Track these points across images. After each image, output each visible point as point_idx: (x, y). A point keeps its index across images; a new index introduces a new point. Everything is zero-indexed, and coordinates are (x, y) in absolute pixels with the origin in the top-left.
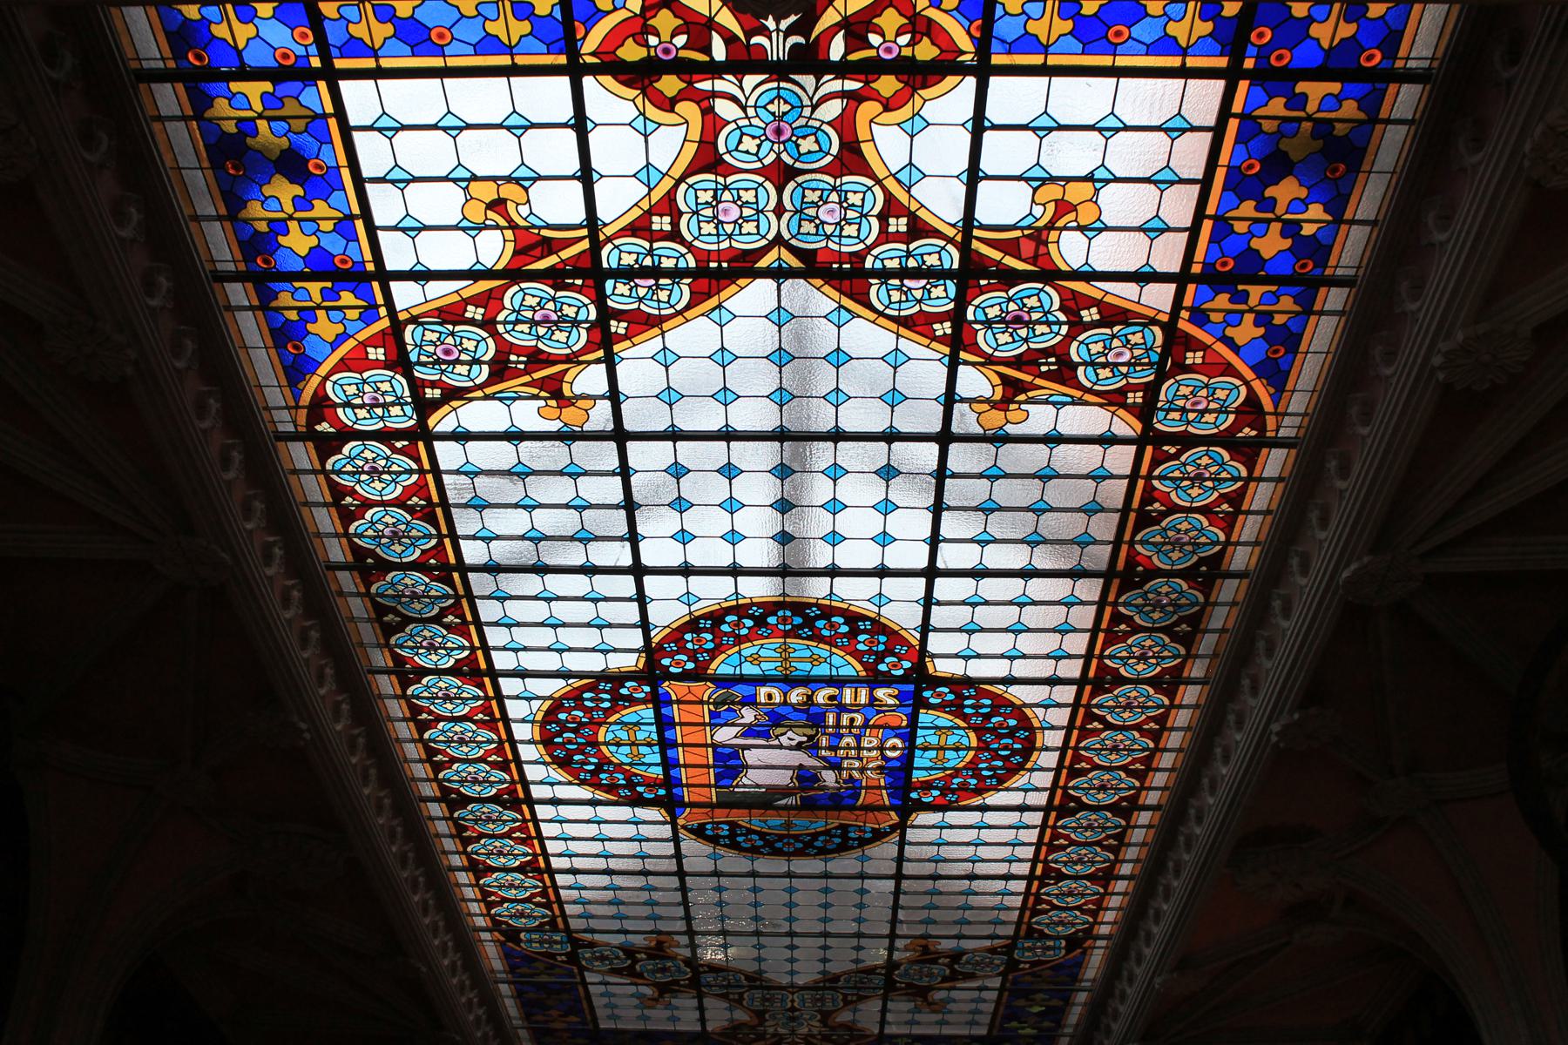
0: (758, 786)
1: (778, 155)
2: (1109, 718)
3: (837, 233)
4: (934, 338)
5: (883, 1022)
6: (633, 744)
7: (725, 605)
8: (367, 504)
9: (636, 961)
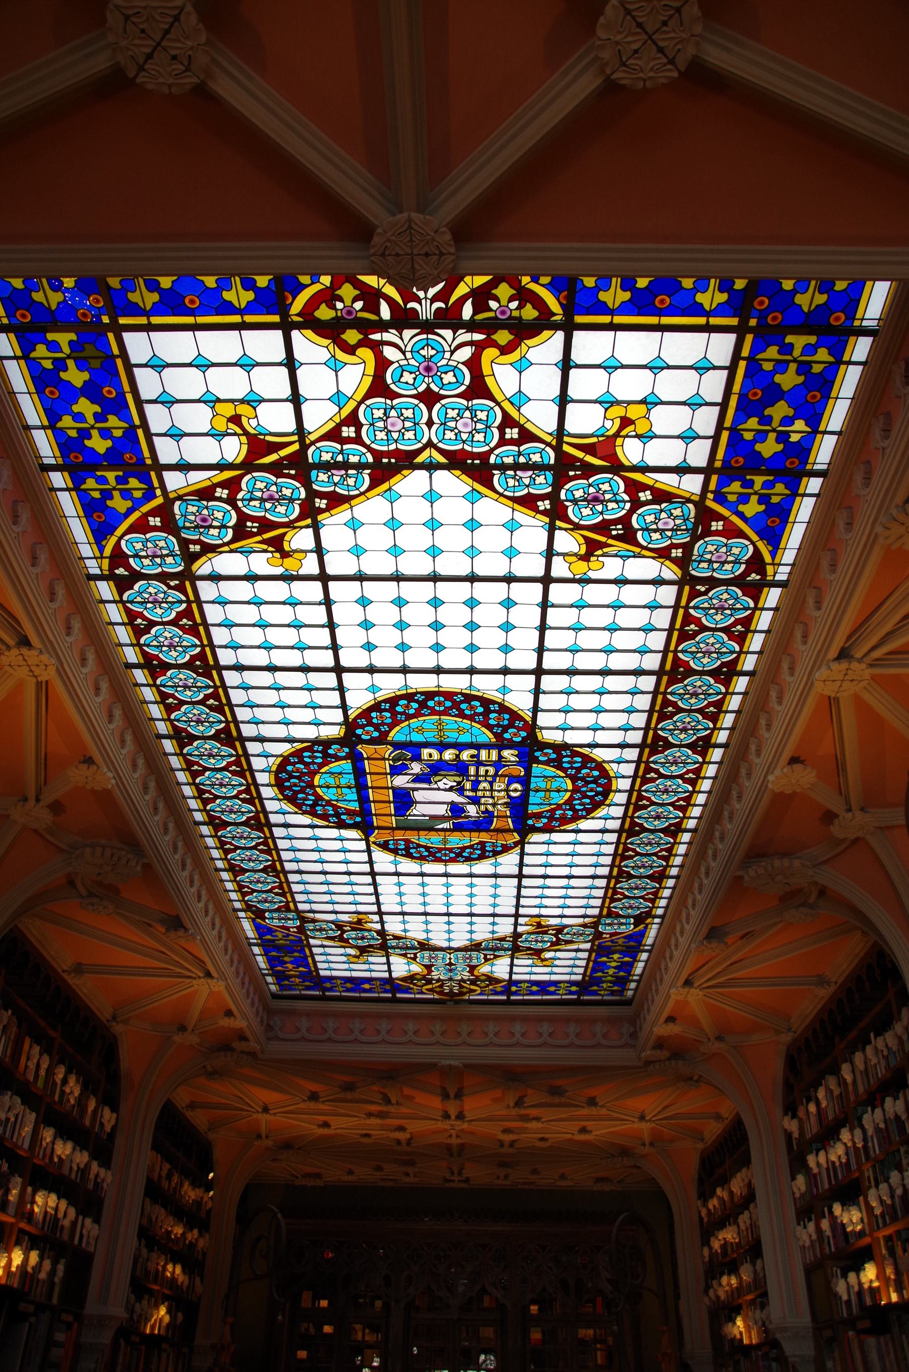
0: (424, 816)
1: (428, 385)
2: (661, 770)
3: (470, 439)
4: (536, 510)
5: (511, 973)
6: (338, 787)
7: (398, 693)
8: (152, 624)
9: (343, 932)
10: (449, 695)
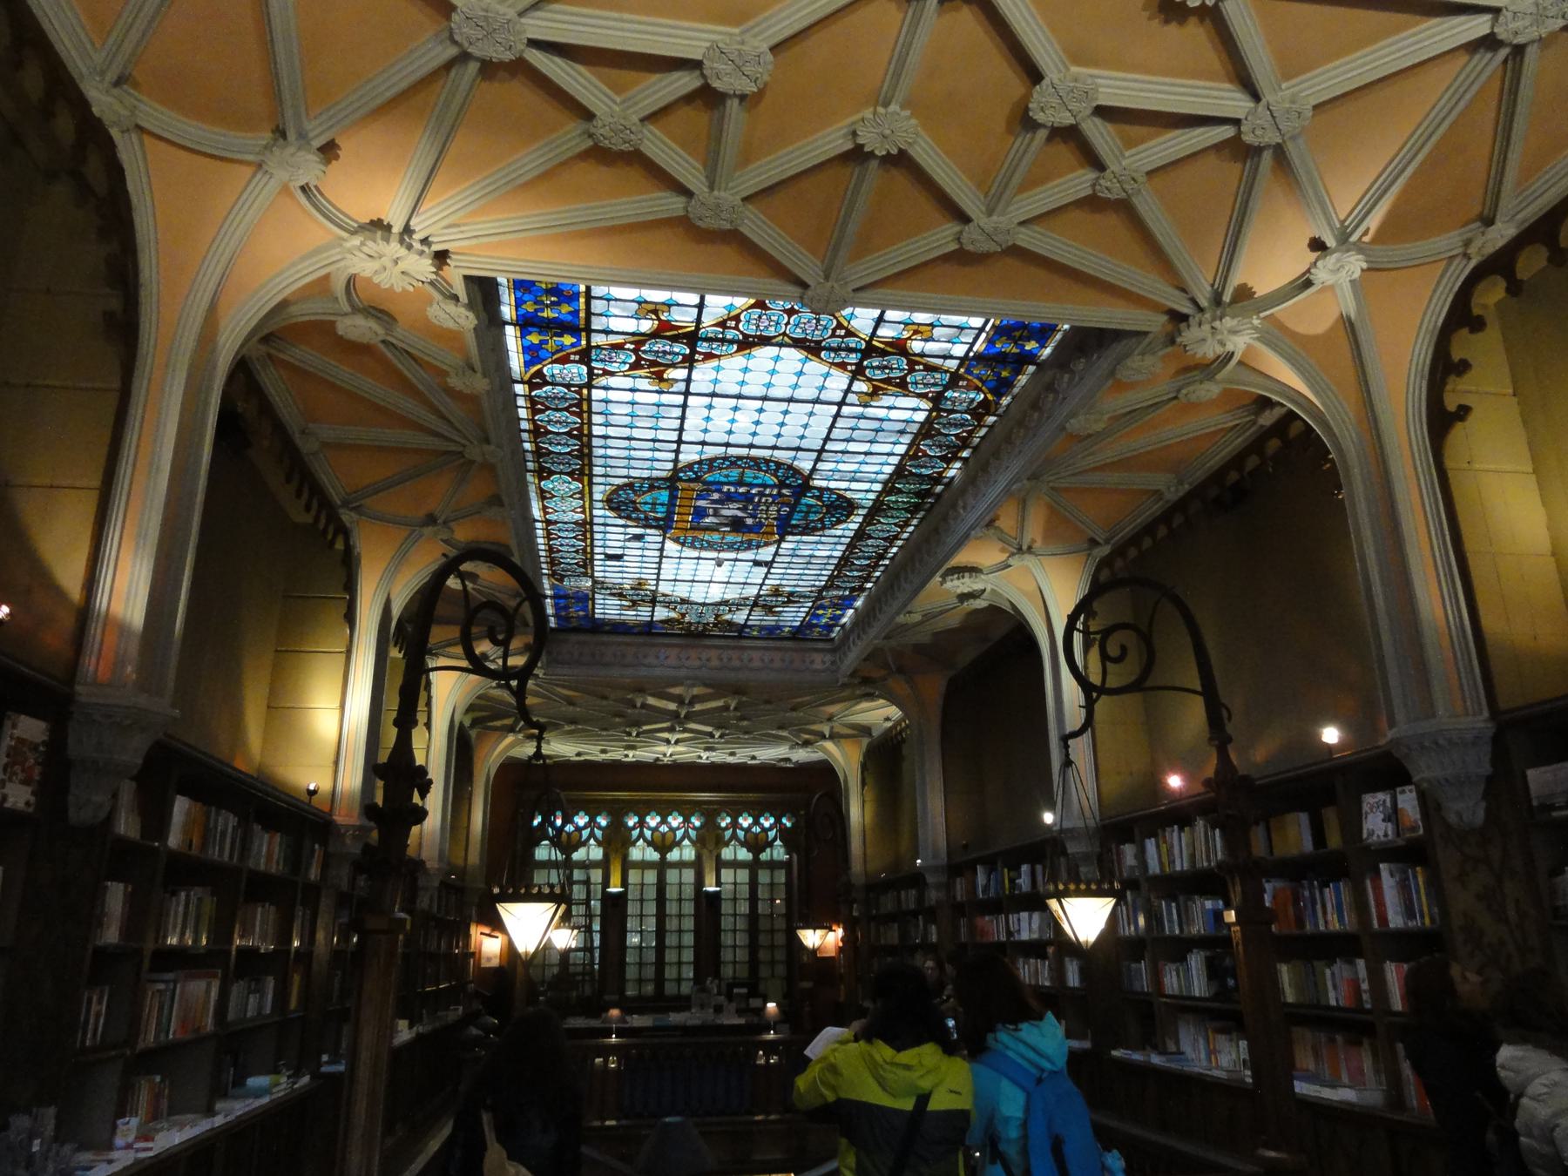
10: (754, 459)
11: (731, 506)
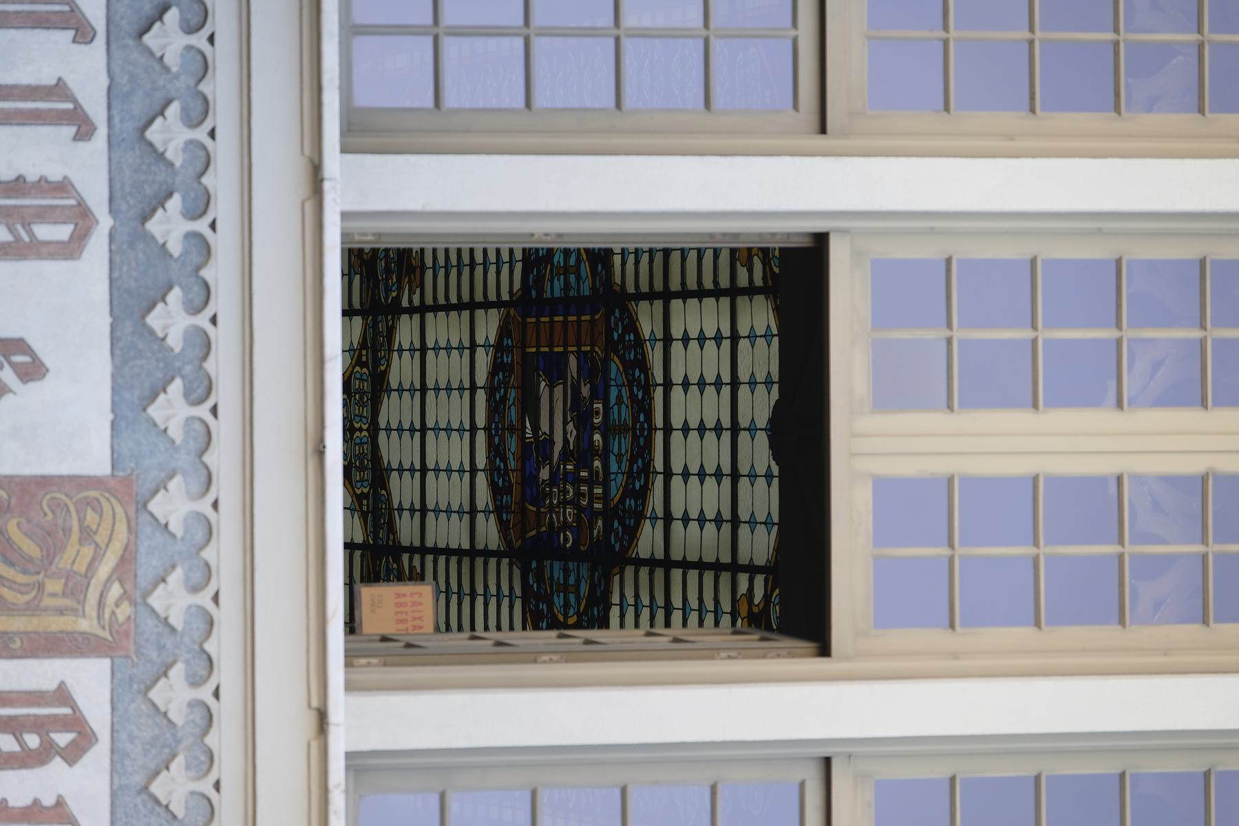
11: (570, 427)
